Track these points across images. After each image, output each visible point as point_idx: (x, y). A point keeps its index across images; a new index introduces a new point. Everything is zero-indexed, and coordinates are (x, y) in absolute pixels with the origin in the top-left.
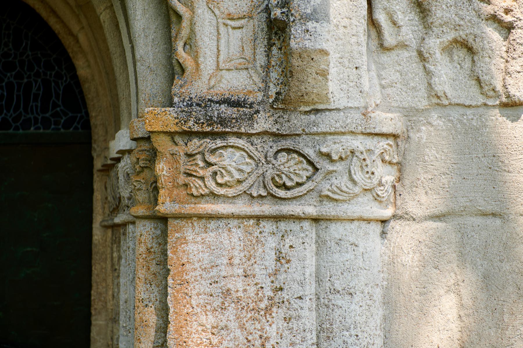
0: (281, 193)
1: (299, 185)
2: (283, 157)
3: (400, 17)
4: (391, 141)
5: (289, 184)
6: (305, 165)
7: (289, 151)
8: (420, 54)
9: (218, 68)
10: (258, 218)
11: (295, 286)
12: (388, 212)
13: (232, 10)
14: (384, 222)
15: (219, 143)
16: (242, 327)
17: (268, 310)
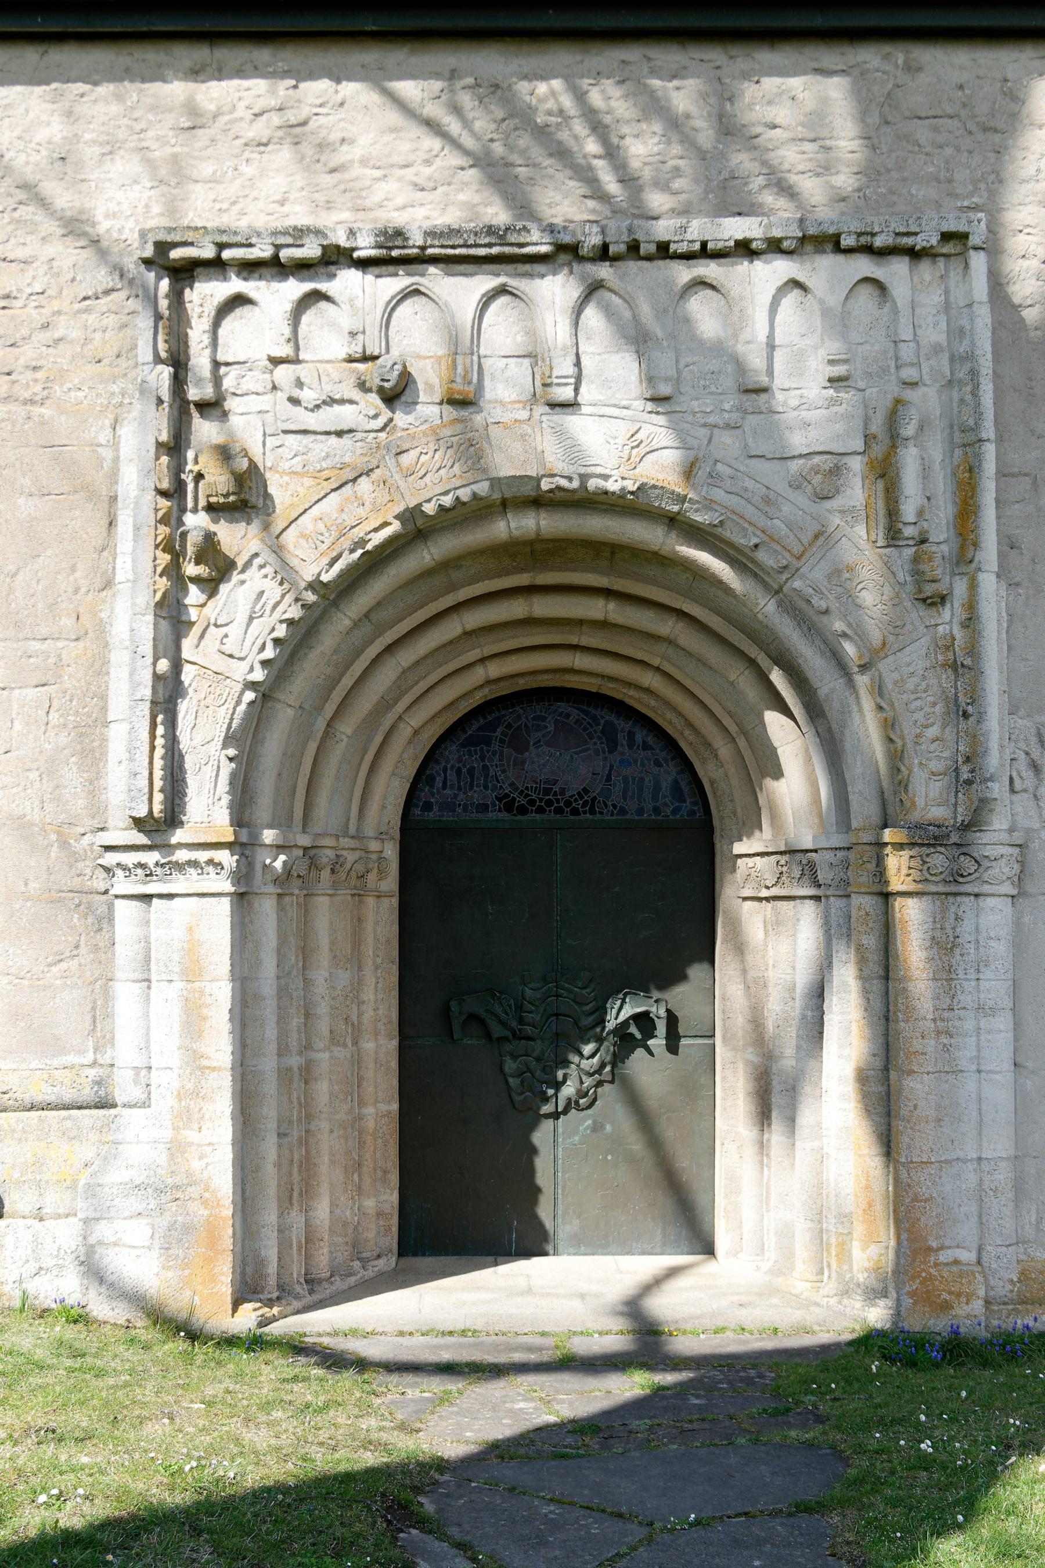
0: (961, 880)
1: (970, 874)
2: (962, 858)
3: (1024, 774)
4: (1018, 850)
5: (965, 874)
6: (973, 862)
7: (964, 854)
8: (1035, 796)
9: (926, 805)
10: (947, 894)
11: (966, 935)
12: (1015, 892)
13: (934, 770)
14: (1013, 897)
15: (932, 850)
16: (940, 959)
17: (951, 949)
